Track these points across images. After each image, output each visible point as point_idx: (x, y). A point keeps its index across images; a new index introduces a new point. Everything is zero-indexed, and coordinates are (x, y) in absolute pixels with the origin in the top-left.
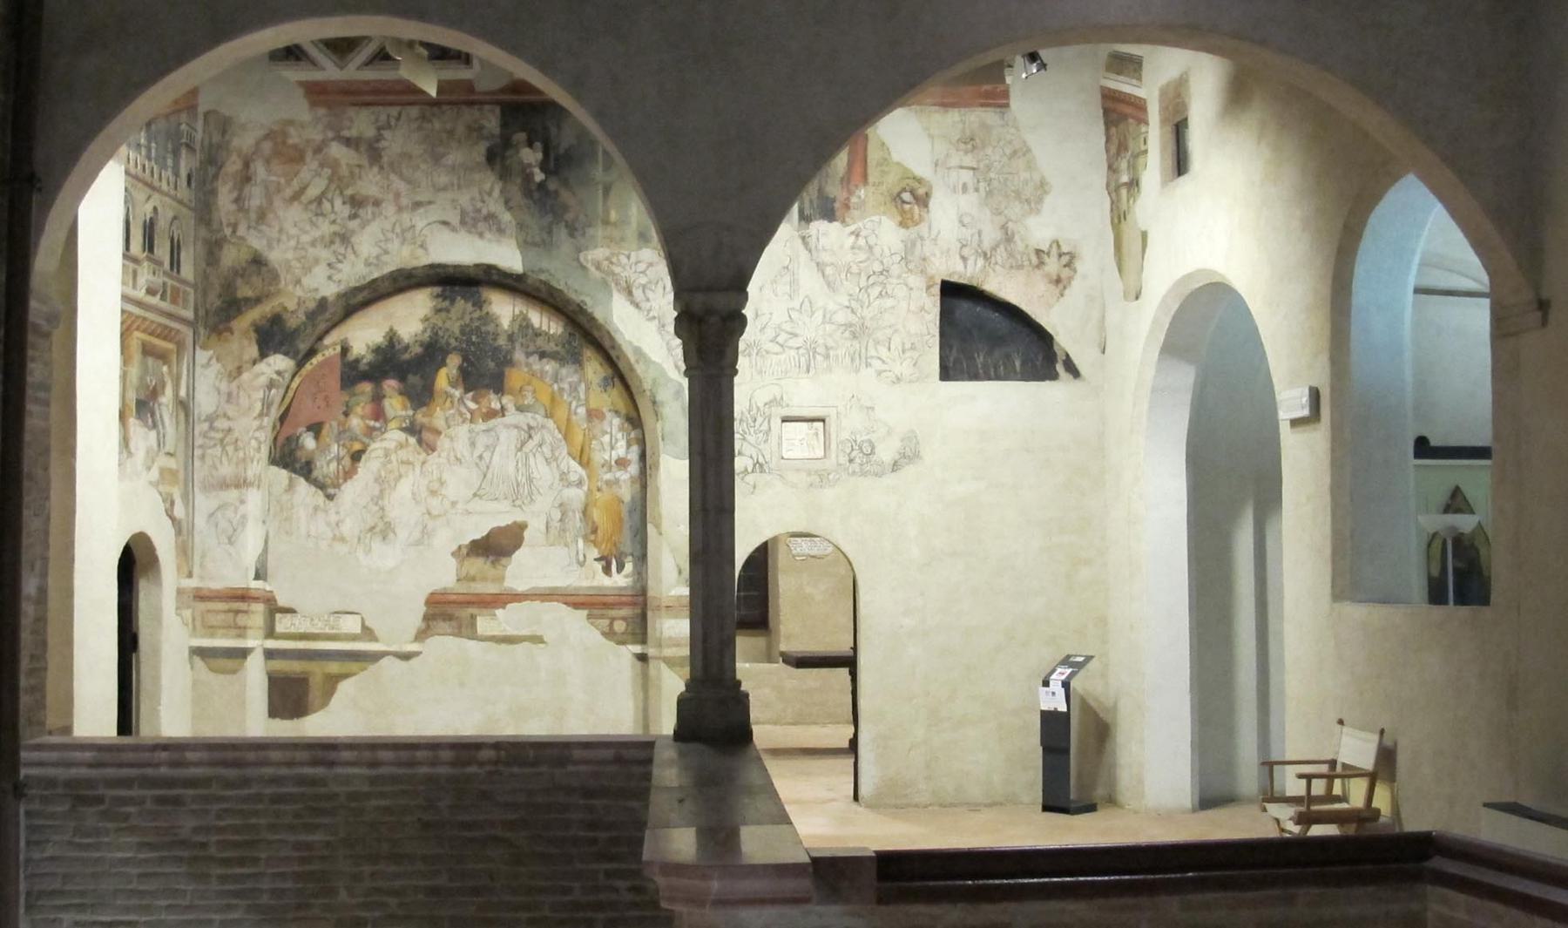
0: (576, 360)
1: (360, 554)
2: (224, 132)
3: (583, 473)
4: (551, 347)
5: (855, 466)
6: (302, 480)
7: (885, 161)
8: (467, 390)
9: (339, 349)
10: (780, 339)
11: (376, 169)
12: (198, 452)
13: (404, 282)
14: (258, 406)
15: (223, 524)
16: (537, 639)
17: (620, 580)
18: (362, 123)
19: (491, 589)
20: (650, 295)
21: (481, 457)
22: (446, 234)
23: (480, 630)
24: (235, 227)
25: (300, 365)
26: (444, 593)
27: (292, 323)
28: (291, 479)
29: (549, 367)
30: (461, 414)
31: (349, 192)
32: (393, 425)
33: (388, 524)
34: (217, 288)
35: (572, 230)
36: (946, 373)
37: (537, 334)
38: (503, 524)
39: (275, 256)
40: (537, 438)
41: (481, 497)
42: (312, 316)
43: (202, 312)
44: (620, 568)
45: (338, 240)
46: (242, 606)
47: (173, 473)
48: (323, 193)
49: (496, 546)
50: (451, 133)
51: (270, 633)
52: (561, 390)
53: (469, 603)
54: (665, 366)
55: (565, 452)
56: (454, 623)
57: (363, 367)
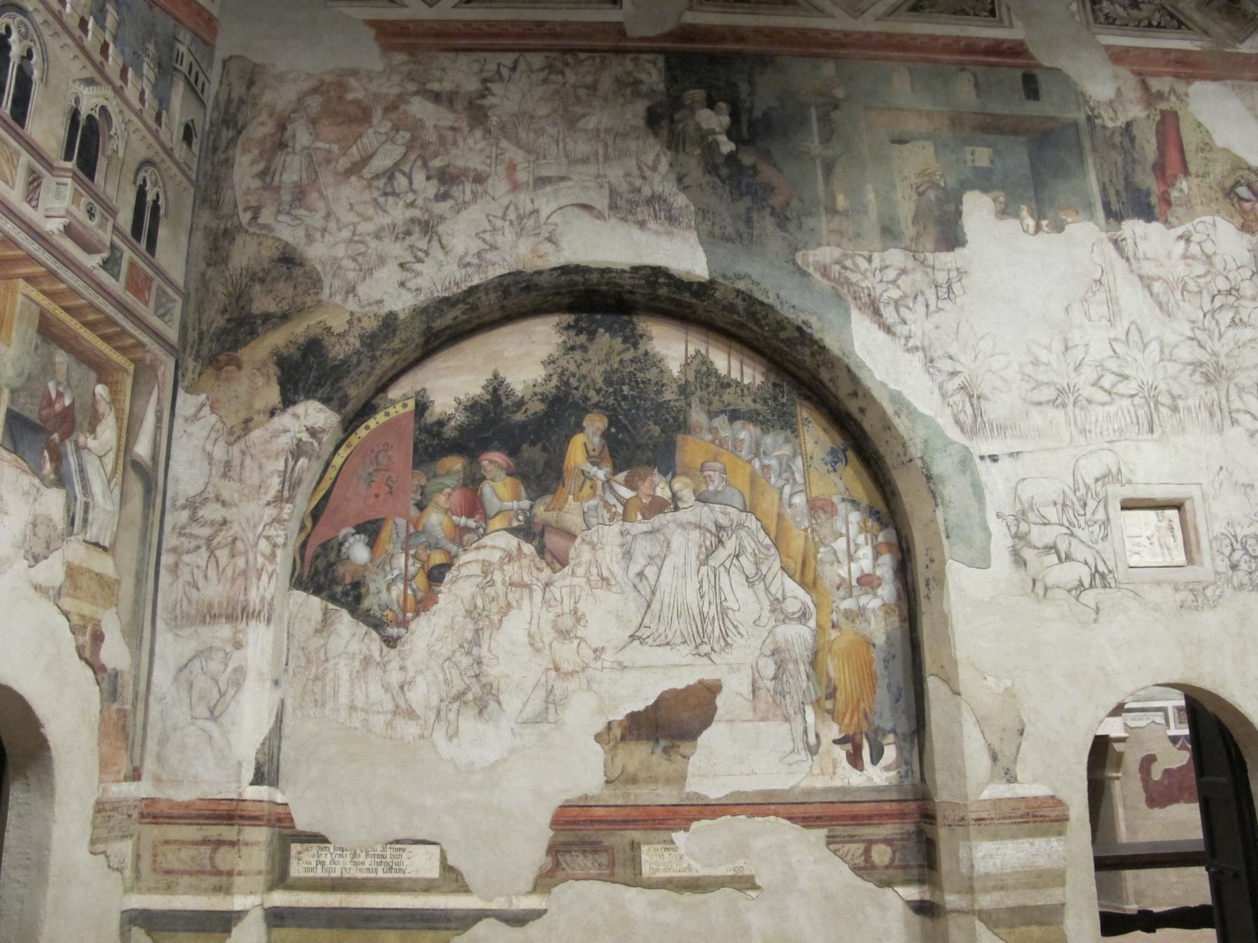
0: (785, 422)
1: (439, 737)
2: (251, 84)
3: (808, 599)
4: (747, 404)
5: (1241, 576)
6: (345, 615)
7: (1206, 146)
8: (617, 469)
9: (411, 404)
10: (1107, 382)
11: (478, 133)
12: (167, 559)
13: (519, 299)
14: (275, 482)
15: (201, 682)
16: (745, 883)
17: (878, 775)
18: (460, 73)
19: (665, 795)
20: (905, 313)
21: (641, 575)
22: (585, 222)
23: (646, 870)
24: (256, 212)
25: (350, 425)
26: (583, 805)
27: (338, 351)
28: (326, 612)
29: (746, 433)
30: (607, 505)
31: (437, 163)
32: (497, 523)
33: (488, 688)
34: (220, 291)
35: (782, 220)
37: (725, 384)
38: (680, 685)
39: (316, 252)
40: (731, 545)
41: (642, 641)
42: (372, 341)
43: (192, 335)
44: (877, 756)
45: (417, 229)
46: (227, 832)
47: (107, 586)
48: (397, 165)
49: (670, 723)
50: (593, 88)
51: (280, 878)
52: (765, 467)
53: (627, 823)
54: (940, 421)
55: (777, 565)
56: (603, 858)
57: (449, 432)
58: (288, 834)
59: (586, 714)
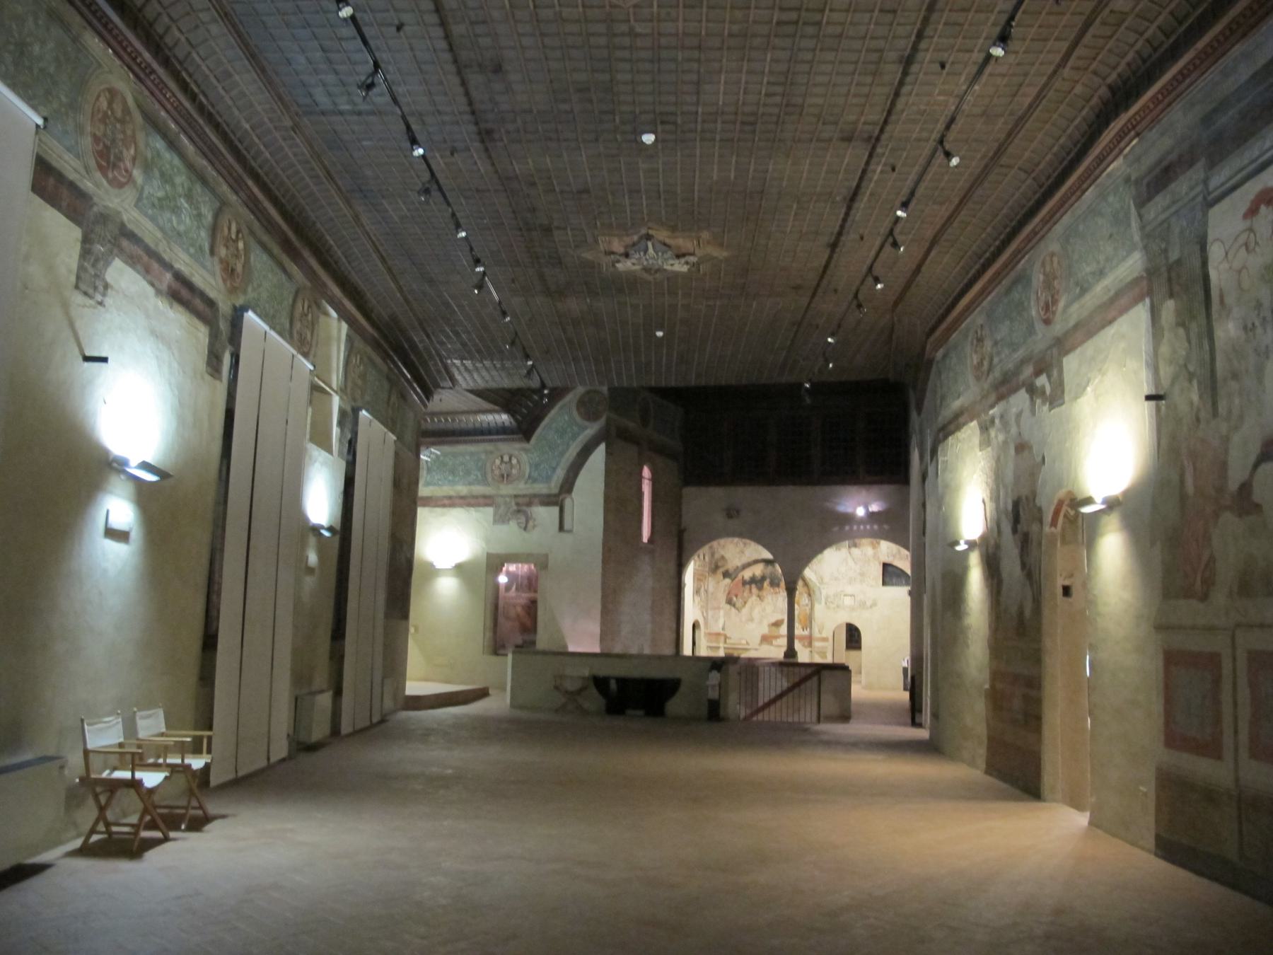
13: (756, 562)
17: (806, 633)
36: (884, 583)
58: (726, 637)
59: (766, 623)
